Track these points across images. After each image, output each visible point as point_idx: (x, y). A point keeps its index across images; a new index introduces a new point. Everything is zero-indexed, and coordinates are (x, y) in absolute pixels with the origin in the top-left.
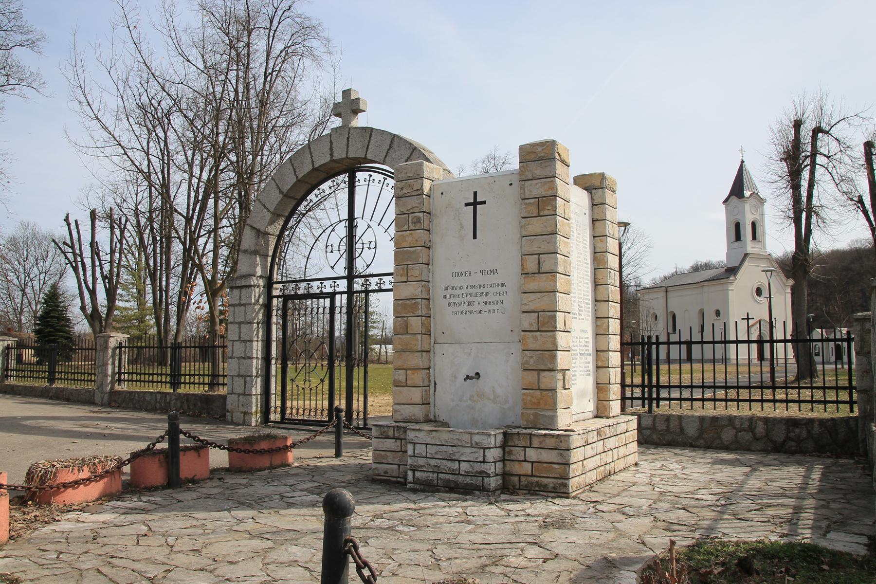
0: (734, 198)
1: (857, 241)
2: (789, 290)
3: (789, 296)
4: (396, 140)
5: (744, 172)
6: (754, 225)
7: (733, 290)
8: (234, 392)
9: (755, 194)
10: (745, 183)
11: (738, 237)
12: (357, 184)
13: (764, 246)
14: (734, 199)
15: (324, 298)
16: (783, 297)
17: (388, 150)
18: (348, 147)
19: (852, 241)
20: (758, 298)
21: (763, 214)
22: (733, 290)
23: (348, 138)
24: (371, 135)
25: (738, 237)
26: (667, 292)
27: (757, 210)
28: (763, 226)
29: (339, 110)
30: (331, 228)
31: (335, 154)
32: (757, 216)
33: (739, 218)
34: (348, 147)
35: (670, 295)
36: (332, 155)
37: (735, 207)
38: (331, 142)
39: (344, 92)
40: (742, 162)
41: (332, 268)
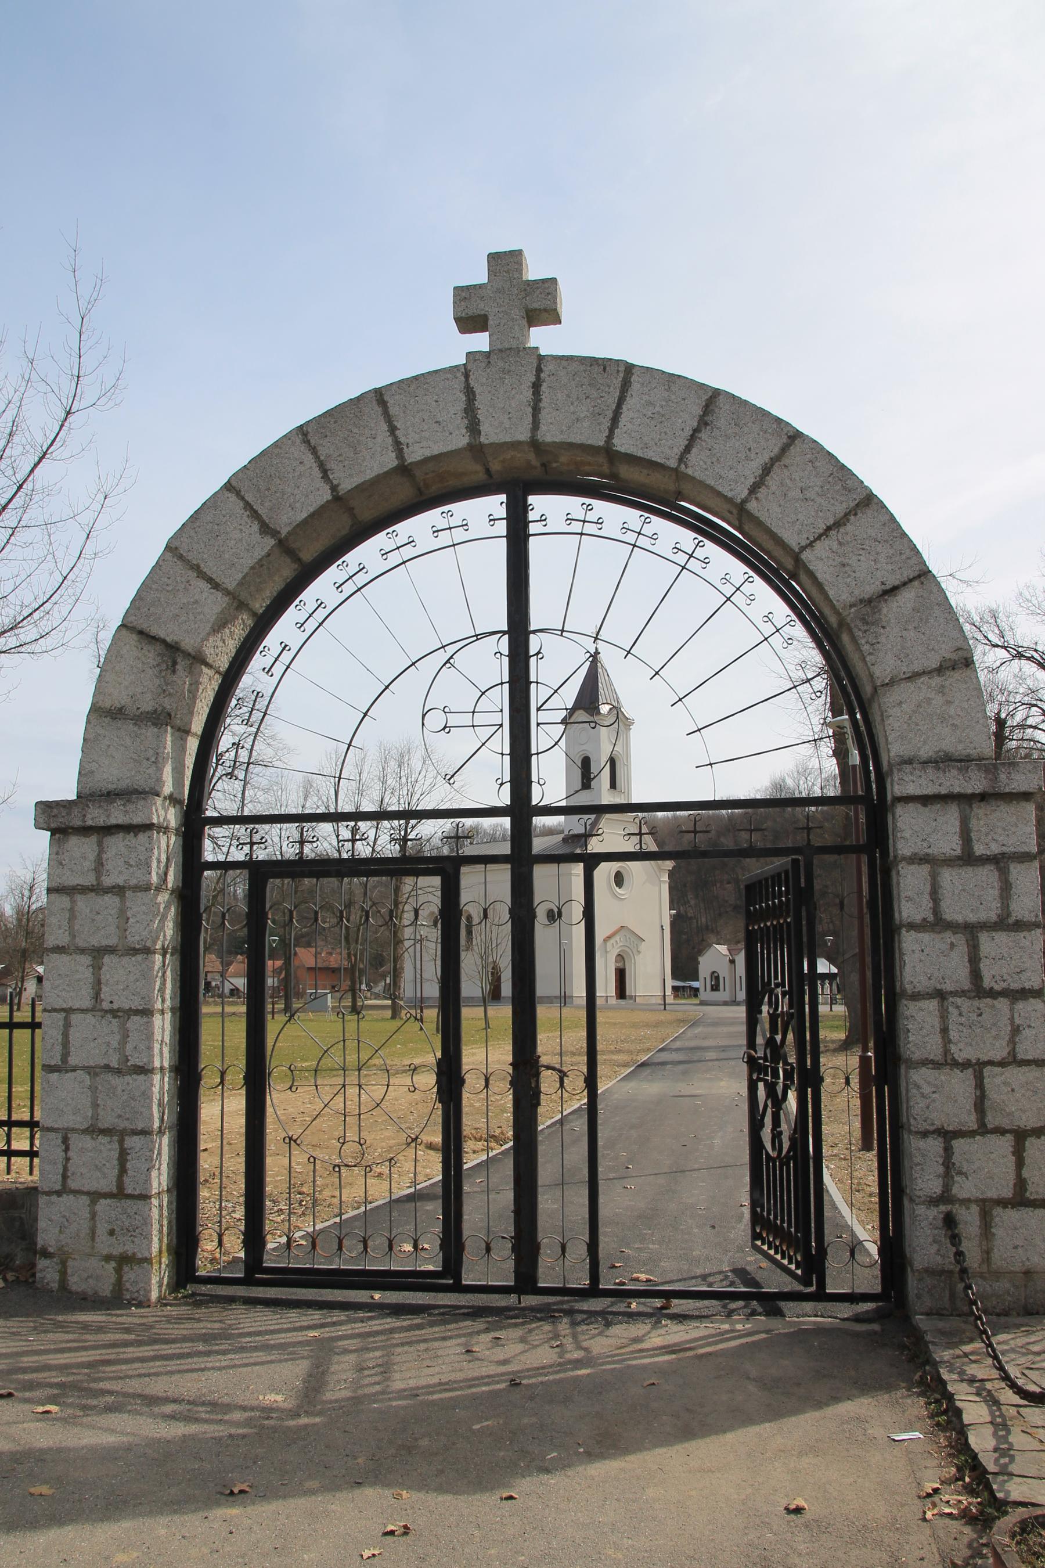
2: (666, 878)
3: (665, 888)
4: (723, 410)
5: (600, 670)
6: (612, 761)
8: (73, 1184)
9: (616, 709)
10: (601, 690)
12: (533, 528)
14: (581, 715)
15: (417, 873)
16: (657, 888)
17: (696, 430)
18: (536, 410)
20: (617, 889)
23: (536, 386)
24: (626, 385)
28: (628, 766)
29: (477, 307)
30: (442, 656)
31: (484, 428)
33: (589, 750)
34: (536, 410)
36: (474, 427)
38: (470, 393)
39: (494, 258)
41: (450, 779)
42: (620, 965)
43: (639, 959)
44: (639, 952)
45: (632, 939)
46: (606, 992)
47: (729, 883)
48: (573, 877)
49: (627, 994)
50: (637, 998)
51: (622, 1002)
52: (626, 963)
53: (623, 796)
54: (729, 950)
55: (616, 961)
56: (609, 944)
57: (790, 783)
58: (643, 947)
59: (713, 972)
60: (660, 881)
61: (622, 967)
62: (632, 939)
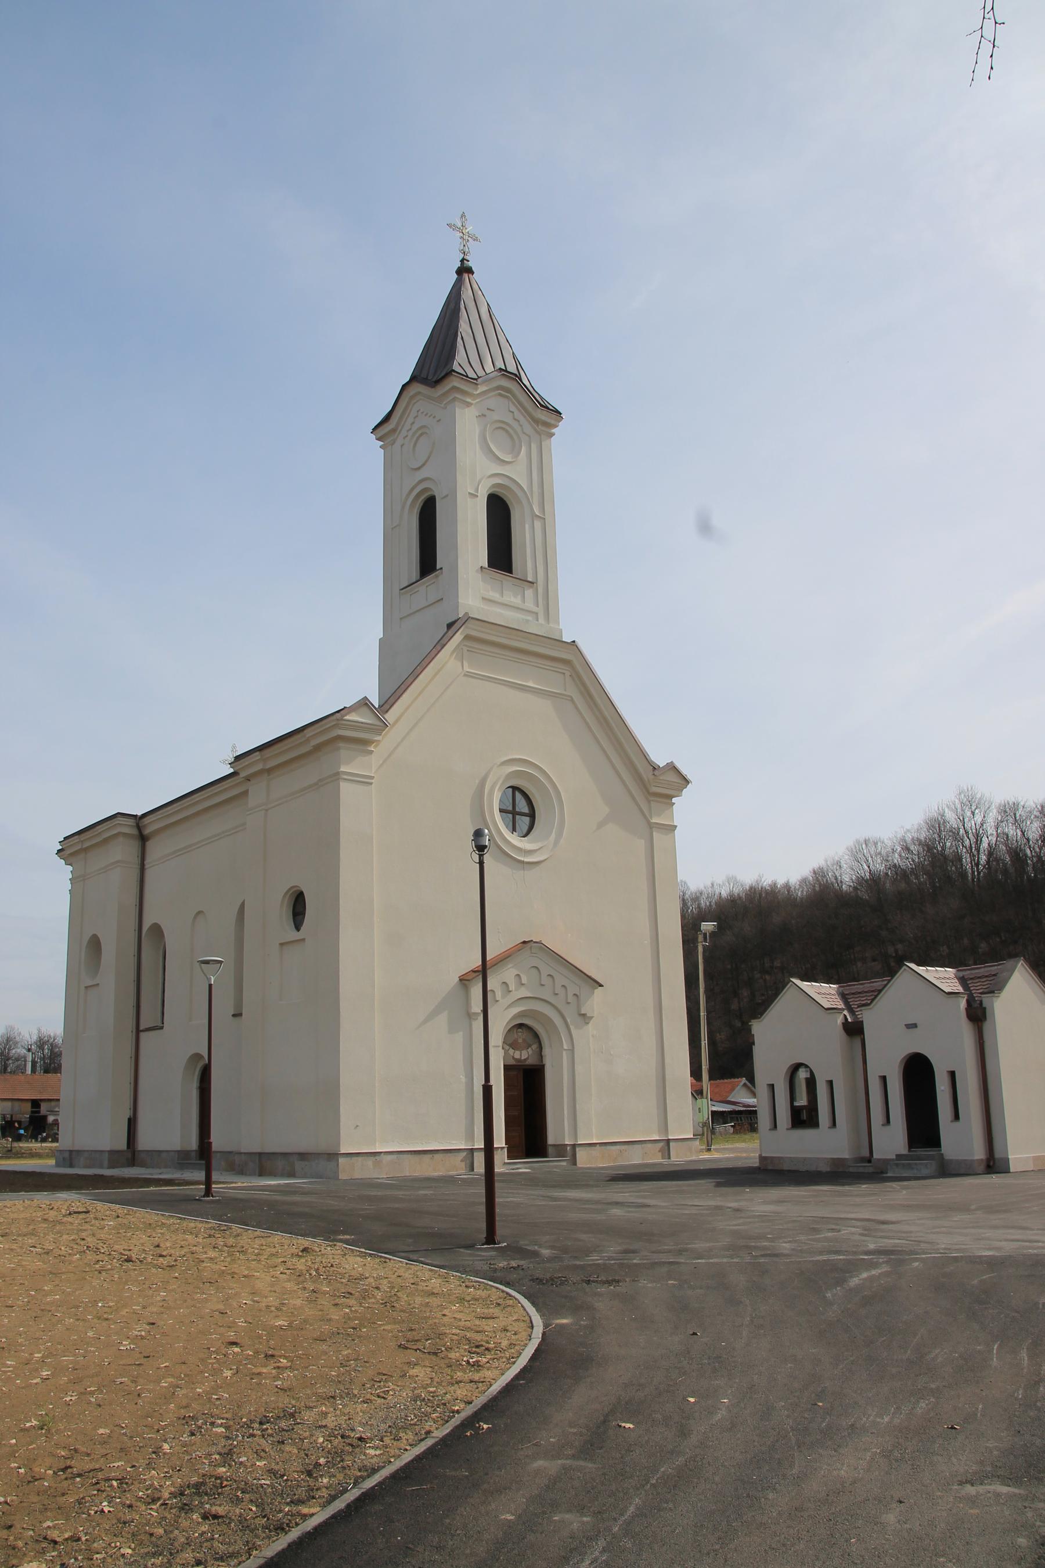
0: (418, 388)
1: (866, 842)
7: (365, 781)
11: (428, 564)
16: (641, 844)
19: (858, 842)
20: (514, 839)
21: (541, 467)
22: (365, 781)
25: (428, 564)
26: (143, 839)
27: (515, 450)
28: (544, 519)
32: (518, 473)
35: (156, 850)
37: (423, 432)
42: (525, 1055)
43: (586, 1038)
44: (585, 1018)
45: (560, 980)
47: (874, 960)
48: (344, 787)
49: (551, 1140)
50: (581, 1155)
52: (546, 1051)
53: (529, 593)
54: (844, 996)
55: (510, 1043)
57: (951, 817)
58: (596, 1002)
59: (796, 1068)
60: (651, 826)
61: (532, 1061)
62: (560, 980)
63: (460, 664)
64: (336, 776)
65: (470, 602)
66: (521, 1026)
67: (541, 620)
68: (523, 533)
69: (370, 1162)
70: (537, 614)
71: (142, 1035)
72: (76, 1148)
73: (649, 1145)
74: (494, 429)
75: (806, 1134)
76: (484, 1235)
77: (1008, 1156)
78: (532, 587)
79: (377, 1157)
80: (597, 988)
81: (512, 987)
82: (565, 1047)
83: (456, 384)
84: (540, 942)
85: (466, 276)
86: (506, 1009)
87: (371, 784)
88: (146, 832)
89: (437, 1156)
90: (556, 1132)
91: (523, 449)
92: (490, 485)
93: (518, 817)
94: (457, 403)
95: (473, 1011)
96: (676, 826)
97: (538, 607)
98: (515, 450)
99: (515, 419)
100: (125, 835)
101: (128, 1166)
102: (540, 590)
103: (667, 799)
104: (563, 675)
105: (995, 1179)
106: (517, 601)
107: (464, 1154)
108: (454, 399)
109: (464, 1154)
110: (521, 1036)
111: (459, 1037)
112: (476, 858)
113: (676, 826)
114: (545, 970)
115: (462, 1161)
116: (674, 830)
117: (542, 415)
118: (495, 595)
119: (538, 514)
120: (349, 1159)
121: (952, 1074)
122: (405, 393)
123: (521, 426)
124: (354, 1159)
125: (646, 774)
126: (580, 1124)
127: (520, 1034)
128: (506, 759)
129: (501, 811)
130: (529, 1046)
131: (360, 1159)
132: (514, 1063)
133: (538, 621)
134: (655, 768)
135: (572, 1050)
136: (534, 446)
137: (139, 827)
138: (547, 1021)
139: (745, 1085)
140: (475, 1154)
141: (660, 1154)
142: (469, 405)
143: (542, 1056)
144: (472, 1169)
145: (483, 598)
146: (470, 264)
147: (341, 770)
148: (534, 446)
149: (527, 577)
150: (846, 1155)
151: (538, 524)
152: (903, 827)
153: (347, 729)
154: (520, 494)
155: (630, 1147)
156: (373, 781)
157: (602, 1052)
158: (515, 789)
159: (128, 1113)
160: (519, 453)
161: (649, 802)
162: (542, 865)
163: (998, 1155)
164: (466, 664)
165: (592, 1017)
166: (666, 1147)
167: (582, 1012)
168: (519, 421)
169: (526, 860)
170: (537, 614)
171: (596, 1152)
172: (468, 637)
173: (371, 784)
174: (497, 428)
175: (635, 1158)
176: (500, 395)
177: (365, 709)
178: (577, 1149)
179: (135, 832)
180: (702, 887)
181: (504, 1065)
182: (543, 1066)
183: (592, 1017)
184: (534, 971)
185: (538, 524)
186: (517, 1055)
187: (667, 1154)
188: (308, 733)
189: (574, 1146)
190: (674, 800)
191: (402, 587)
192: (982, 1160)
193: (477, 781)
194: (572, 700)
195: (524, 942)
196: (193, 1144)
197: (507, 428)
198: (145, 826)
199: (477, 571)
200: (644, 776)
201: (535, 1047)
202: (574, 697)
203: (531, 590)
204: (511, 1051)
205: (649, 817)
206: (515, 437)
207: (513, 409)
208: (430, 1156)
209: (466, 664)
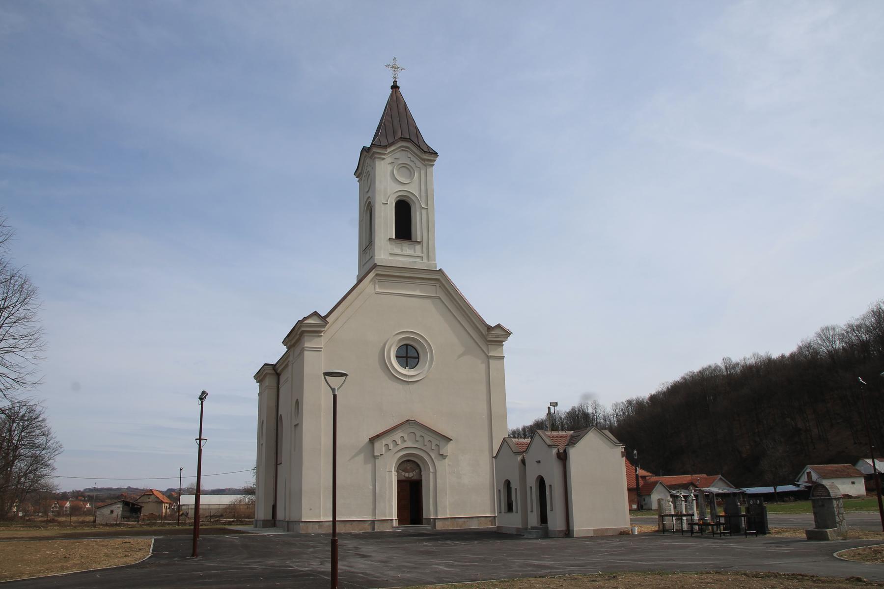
7: (318, 350)
13: (429, 253)
16: (483, 367)
22: (318, 350)
26: (278, 375)
32: (413, 189)
40: (395, 87)
43: (443, 467)
44: (443, 457)
46: (374, 514)
48: (307, 354)
49: (425, 516)
51: (412, 528)
52: (423, 473)
53: (418, 247)
56: (379, 446)
60: (489, 358)
62: (427, 438)
63: (373, 286)
64: (303, 350)
65: (382, 257)
66: (408, 461)
67: (425, 260)
68: (418, 219)
69: (317, 526)
70: (422, 257)
71: (278, 466)
72: (291, 520)
73: (483, 519)
74: (399, 168)
75: (510, 515)
76: (191, 551)
77: (573, 528)
78: (420, 244)
79: (321, 523)
80: (449, 442)
81: (399, 442)
82: (431, 470)
83: (374, 150)
84: (415, 420)
85: (394, 90)
86: (396, 453)
87: (321, 351)
88: (279, 371)
89: (354, 523)
90: (429, 512)
91: (416, 174)
92: (396, 196)
93: (408, 359)
94: (376, 159)
95: (375, 454)
96: (504, 356)
97: (423, 253)
98: (411, 175)
99: (412, 161)
100: (269, 373)
101: (272, 527)
102: (425, 245)
103: (500, 343)
104: (435, 287)
105: (569, 540)
106: (410, 252)
107: (370, 522)
108: (376, 158)
109: (370, 522)
110: (409, 466)
111: (369, 467)
112: (200, 402)
113: (504, 356)
114: (418, 434)
115: (368, 526)
116: (503, 358)
117: (426, 157)
118: (397, 251)
119: (423, 206)
120: (305, 524)
121: (550, 486)
122: (362, 155)
123: (415, 164)
124: (308, 524)
125: (484, 330)
126: (439, 508)
127: (409, 465)
128: (399, 332)
129: (397, 357)
130: (414, 470)
131: (311, 524)
132: (405, 479)
133: (423, 260)
134: (489, 328)
135: (435, 472)
136: (423, 172)
137: (274, 369)
138: (422, 458)
139: (721, 479)
140: (376, 522)
141: (490, 523)
142: (383, 159)
143: (421, 475)
144: (374, 529)
145: (390, 254)
146: (398, 85)
147: (305, 346)
148: (423, 172)
149: (416, 238)
150: (520, 526)
151: (424, 212)
152: (853, 318)
153: (306, 327)
154: (413, 198)
155: (471, 519)
156: (322, 350)
157: (454, 473)
158: (407, 345)
159: (272, 503)
160: (413, 177)
161: (488, 345)
162: (418, 383)
163: (571, 529)
164: (377, 286)
165: (447, 456)
166: (494, 520)
167: (441, 453)
168: (413, 161)
169: (409, 380)
170: (422, 257)
171: (448, 522)
172: (377, 275)
173: (321, 351)
174: (401, 167)
175: (474, 525)
176: (403, 150)
177: (315, 317)
178: (436, 521)
179: (273, 372)
180: (738, 361)
181: (398, 481)
182: (421, 480)
183: (447, 456)
184: (413, 434)
185: (424, 212)
186: (407, 476)
187: (494, 523)
188: (296, 329)
189: (435, 519)
190: (503, 343)
191: (364, 248)
192: (562, 530)
193: (382, 344)
194: (440, 298)
195: (408, 420)
196: (270, 517)
197: (407, 166)
198: (278, 369)
199: (387, 241)
200: (483, 332)
201: (417, 471)
202: (441, 297)
203: (420, 245)
204: (403, 473)
205: (487, 353)
206: (412, 170)
207: (410, 156)
208: (351, 523)
209: (377, 286)
